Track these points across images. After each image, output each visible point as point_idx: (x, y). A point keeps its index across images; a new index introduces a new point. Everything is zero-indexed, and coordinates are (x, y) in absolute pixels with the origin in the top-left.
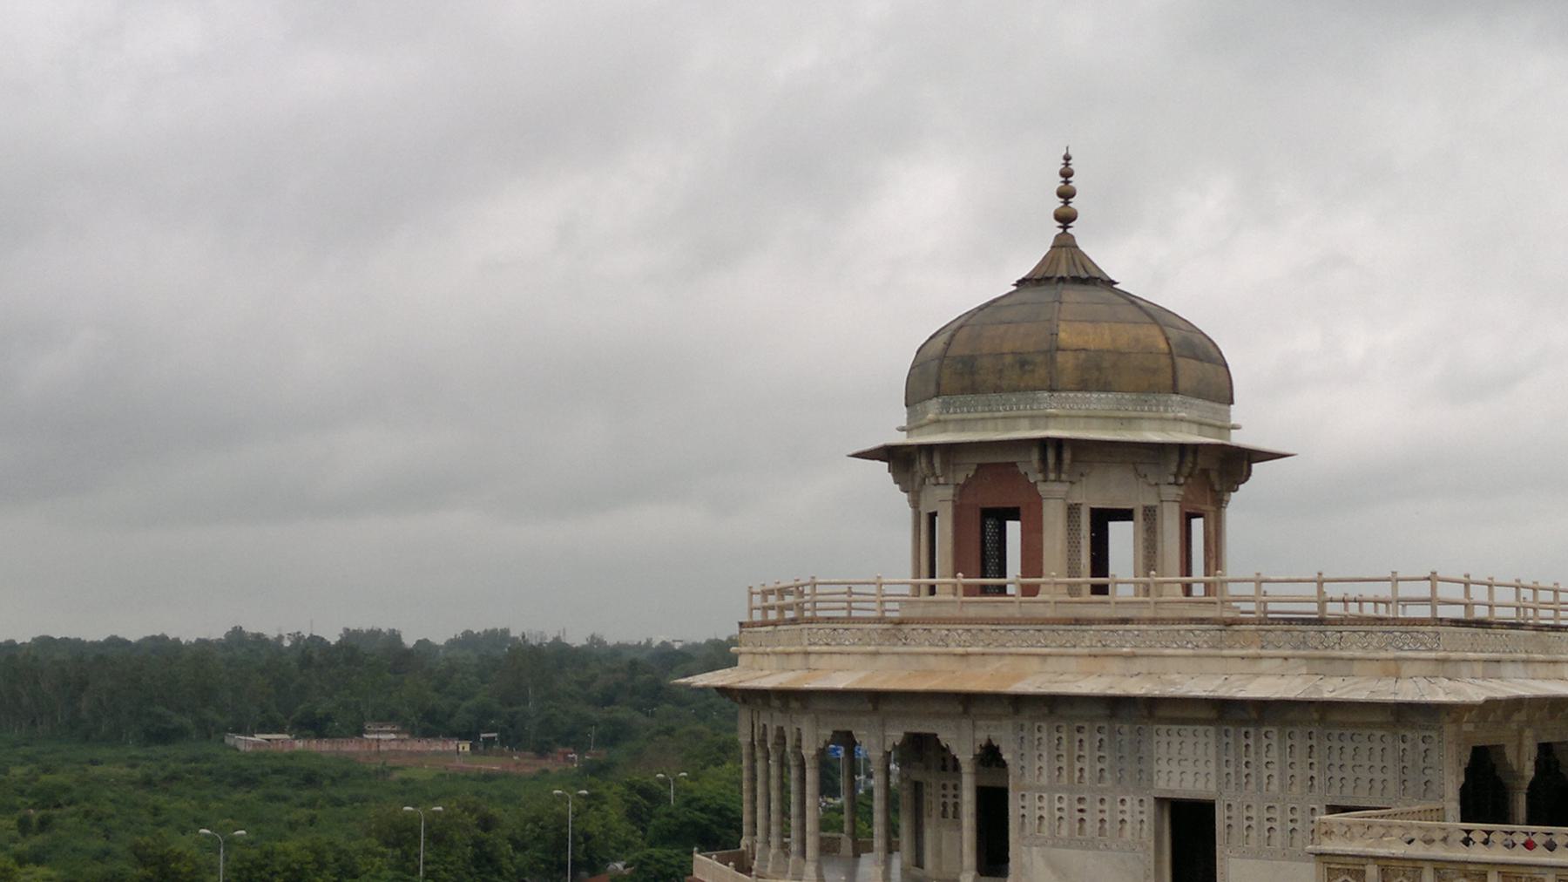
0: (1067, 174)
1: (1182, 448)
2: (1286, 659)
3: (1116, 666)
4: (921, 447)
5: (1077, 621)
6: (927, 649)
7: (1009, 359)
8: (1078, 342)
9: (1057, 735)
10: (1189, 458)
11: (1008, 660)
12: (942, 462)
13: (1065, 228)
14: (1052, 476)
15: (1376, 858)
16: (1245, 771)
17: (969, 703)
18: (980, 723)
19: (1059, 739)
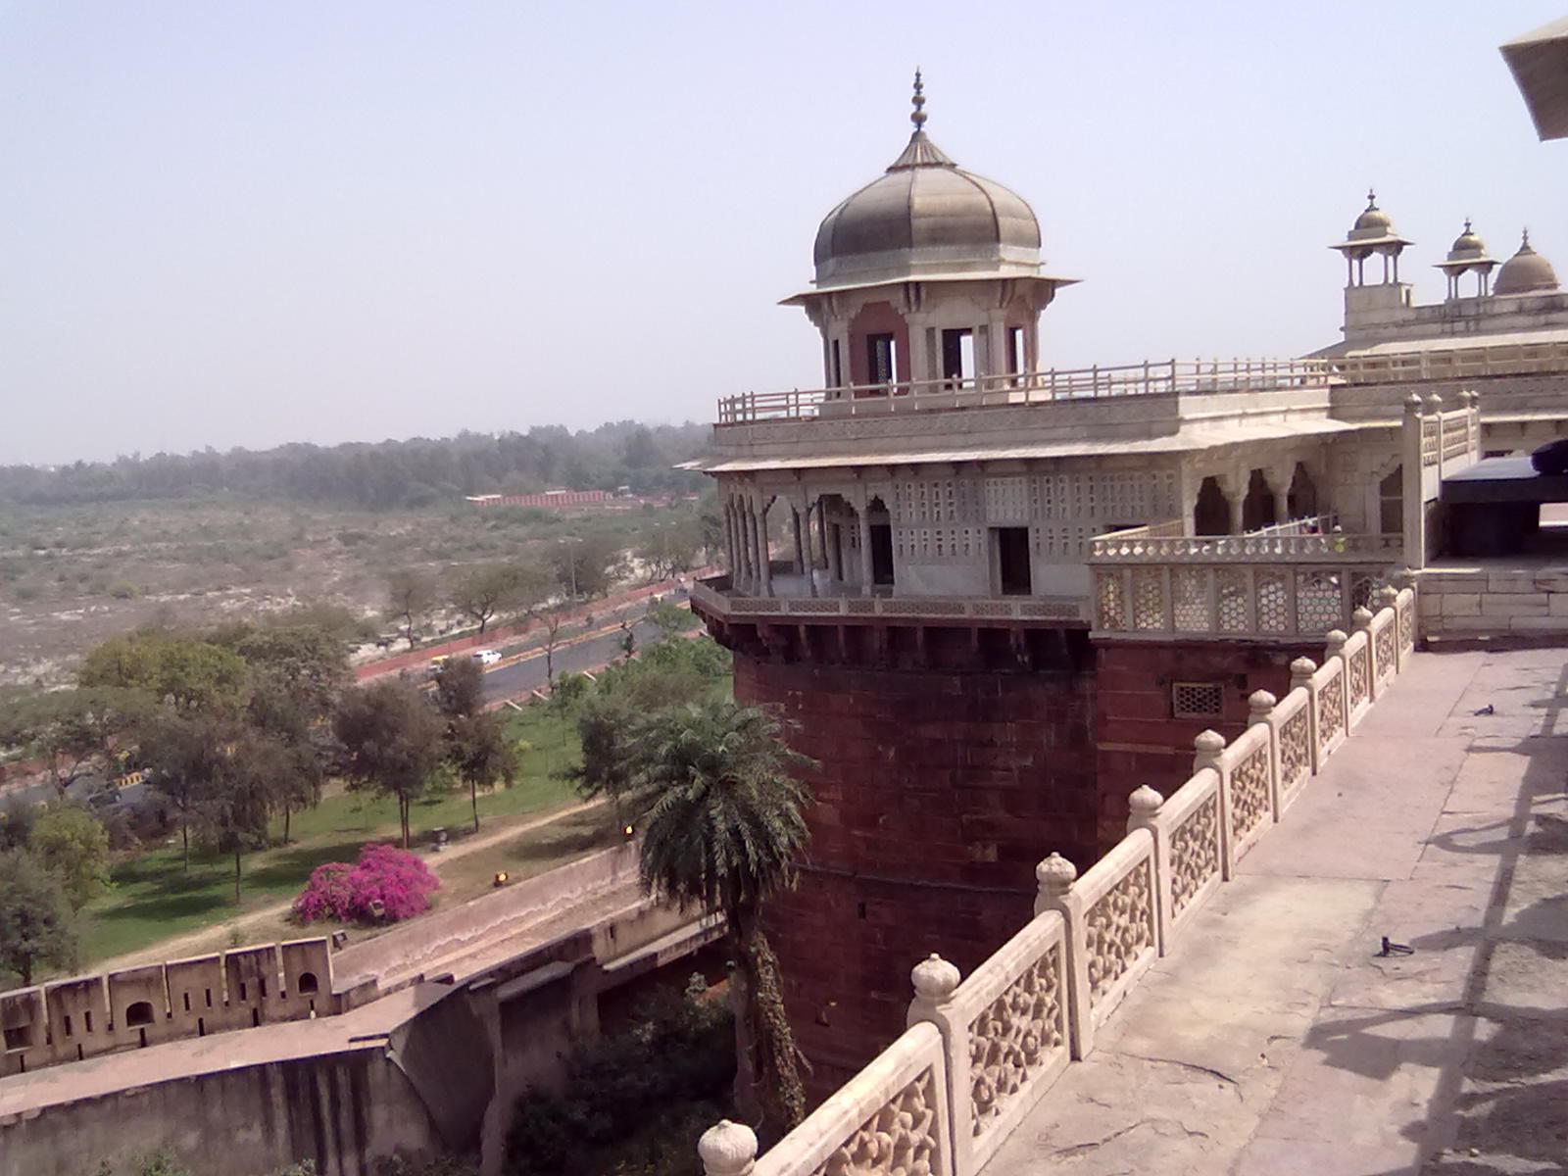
0: (918, 86)
1: (1004, 281)
2: (1073, 427)
4: (823, 294)
10: (1009, 287)
13: (919, 126)
18: (870, 485)
19: (923, 493)
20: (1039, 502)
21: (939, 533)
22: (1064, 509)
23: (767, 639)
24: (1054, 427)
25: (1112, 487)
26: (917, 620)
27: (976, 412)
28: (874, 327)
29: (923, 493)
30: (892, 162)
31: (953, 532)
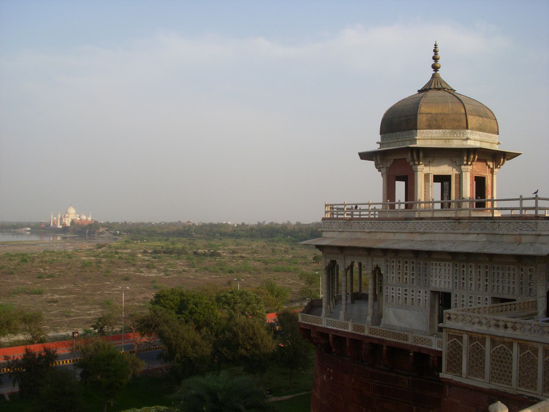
3: (418, 237)
5: (406, 219)
6: (358, 230)
8: (429, 110)
9: (399, 264)
11: (383, 234)
15: (467, 331)
16: (462, 281)
17: (369, 251)
18: (375, 259)
20: (458, 278)
22: (471, 284)
26: (383, 340)
27: (428, 221)
29: (399, 266)
31: (413, 291)
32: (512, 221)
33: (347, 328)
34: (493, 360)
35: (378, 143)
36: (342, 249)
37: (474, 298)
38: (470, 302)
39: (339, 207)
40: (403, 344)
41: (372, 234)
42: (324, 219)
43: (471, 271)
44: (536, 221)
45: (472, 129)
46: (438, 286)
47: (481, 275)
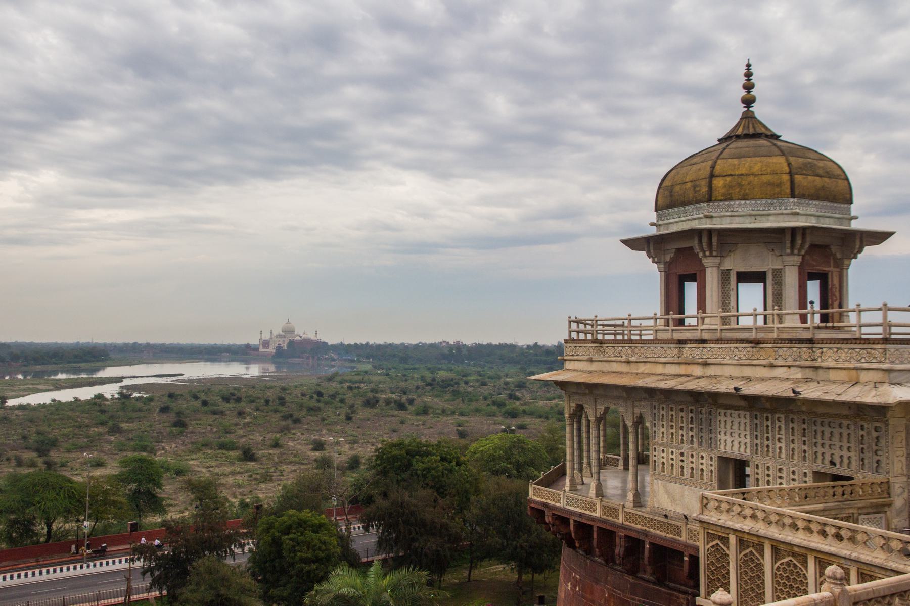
0: (748, 75)
1: (794, 230)
2: (789, 367)
6: (613, 359)
7: (689, 185)
11: (648, 365)
12: (654, 249)
14: (707, 253)
15: (735, 531)
16: (766, 443)
18: (636, 403)
21: (682, 454)
22: (780, 448)
23: (553, 525)
24: (772, 366)
25: (823, 432)
26: (646, 534)
28: (682, 270)
30: (721, 135)
31: (692, 456)
32: (843, 346)
33: (594, 511)
34: (778, 583)
35: (652, 224)
36: (591, 389)
37: (785, 471)
38: (780, 477)
39: (606, 322)
40: (673, 541)
41: (633, 365)
42: (566, 341)
43: (779, 427)
44: (883, 346)
45: (802, 196)
46: (728, 449)
47: (796, 434)
